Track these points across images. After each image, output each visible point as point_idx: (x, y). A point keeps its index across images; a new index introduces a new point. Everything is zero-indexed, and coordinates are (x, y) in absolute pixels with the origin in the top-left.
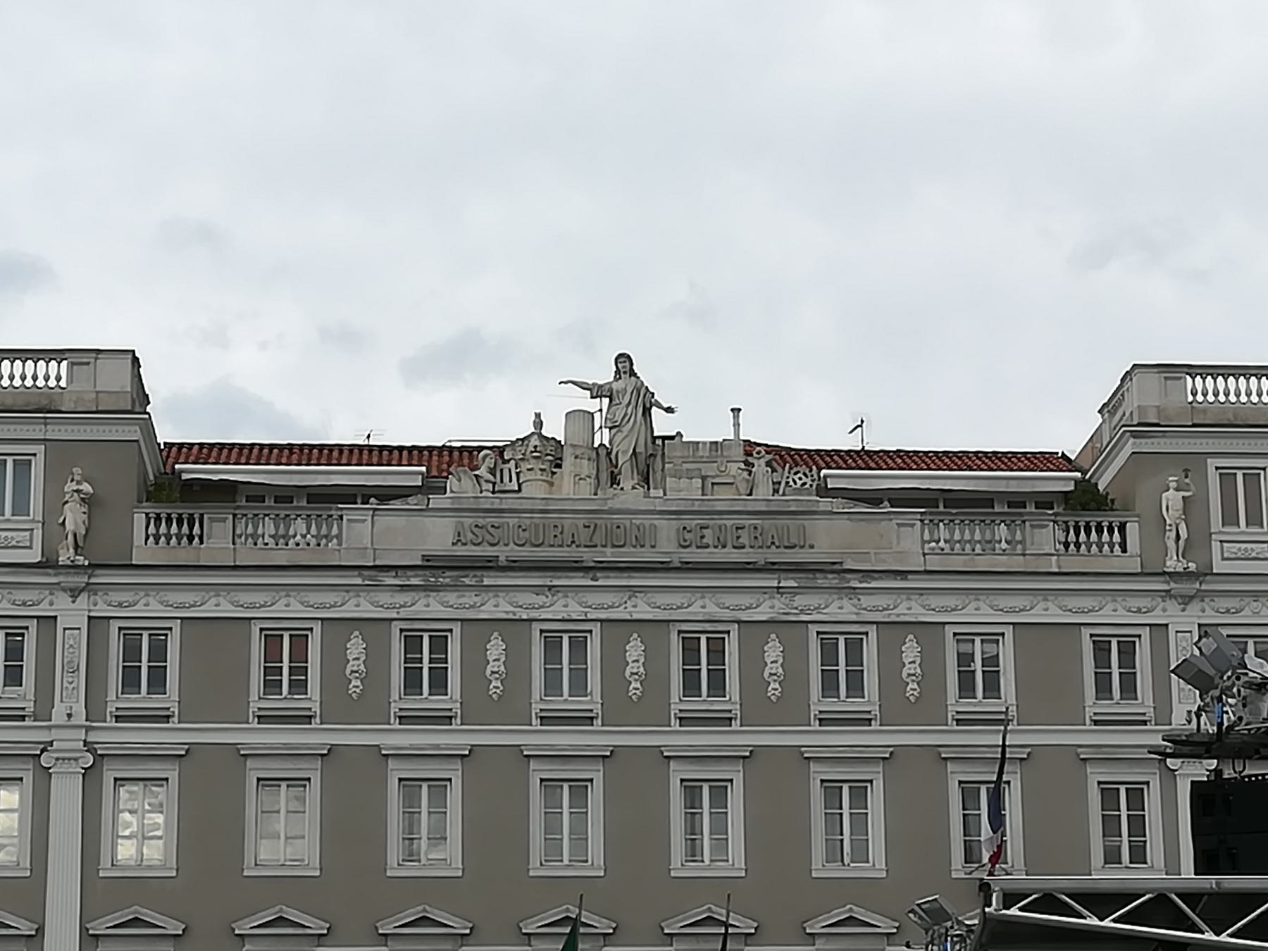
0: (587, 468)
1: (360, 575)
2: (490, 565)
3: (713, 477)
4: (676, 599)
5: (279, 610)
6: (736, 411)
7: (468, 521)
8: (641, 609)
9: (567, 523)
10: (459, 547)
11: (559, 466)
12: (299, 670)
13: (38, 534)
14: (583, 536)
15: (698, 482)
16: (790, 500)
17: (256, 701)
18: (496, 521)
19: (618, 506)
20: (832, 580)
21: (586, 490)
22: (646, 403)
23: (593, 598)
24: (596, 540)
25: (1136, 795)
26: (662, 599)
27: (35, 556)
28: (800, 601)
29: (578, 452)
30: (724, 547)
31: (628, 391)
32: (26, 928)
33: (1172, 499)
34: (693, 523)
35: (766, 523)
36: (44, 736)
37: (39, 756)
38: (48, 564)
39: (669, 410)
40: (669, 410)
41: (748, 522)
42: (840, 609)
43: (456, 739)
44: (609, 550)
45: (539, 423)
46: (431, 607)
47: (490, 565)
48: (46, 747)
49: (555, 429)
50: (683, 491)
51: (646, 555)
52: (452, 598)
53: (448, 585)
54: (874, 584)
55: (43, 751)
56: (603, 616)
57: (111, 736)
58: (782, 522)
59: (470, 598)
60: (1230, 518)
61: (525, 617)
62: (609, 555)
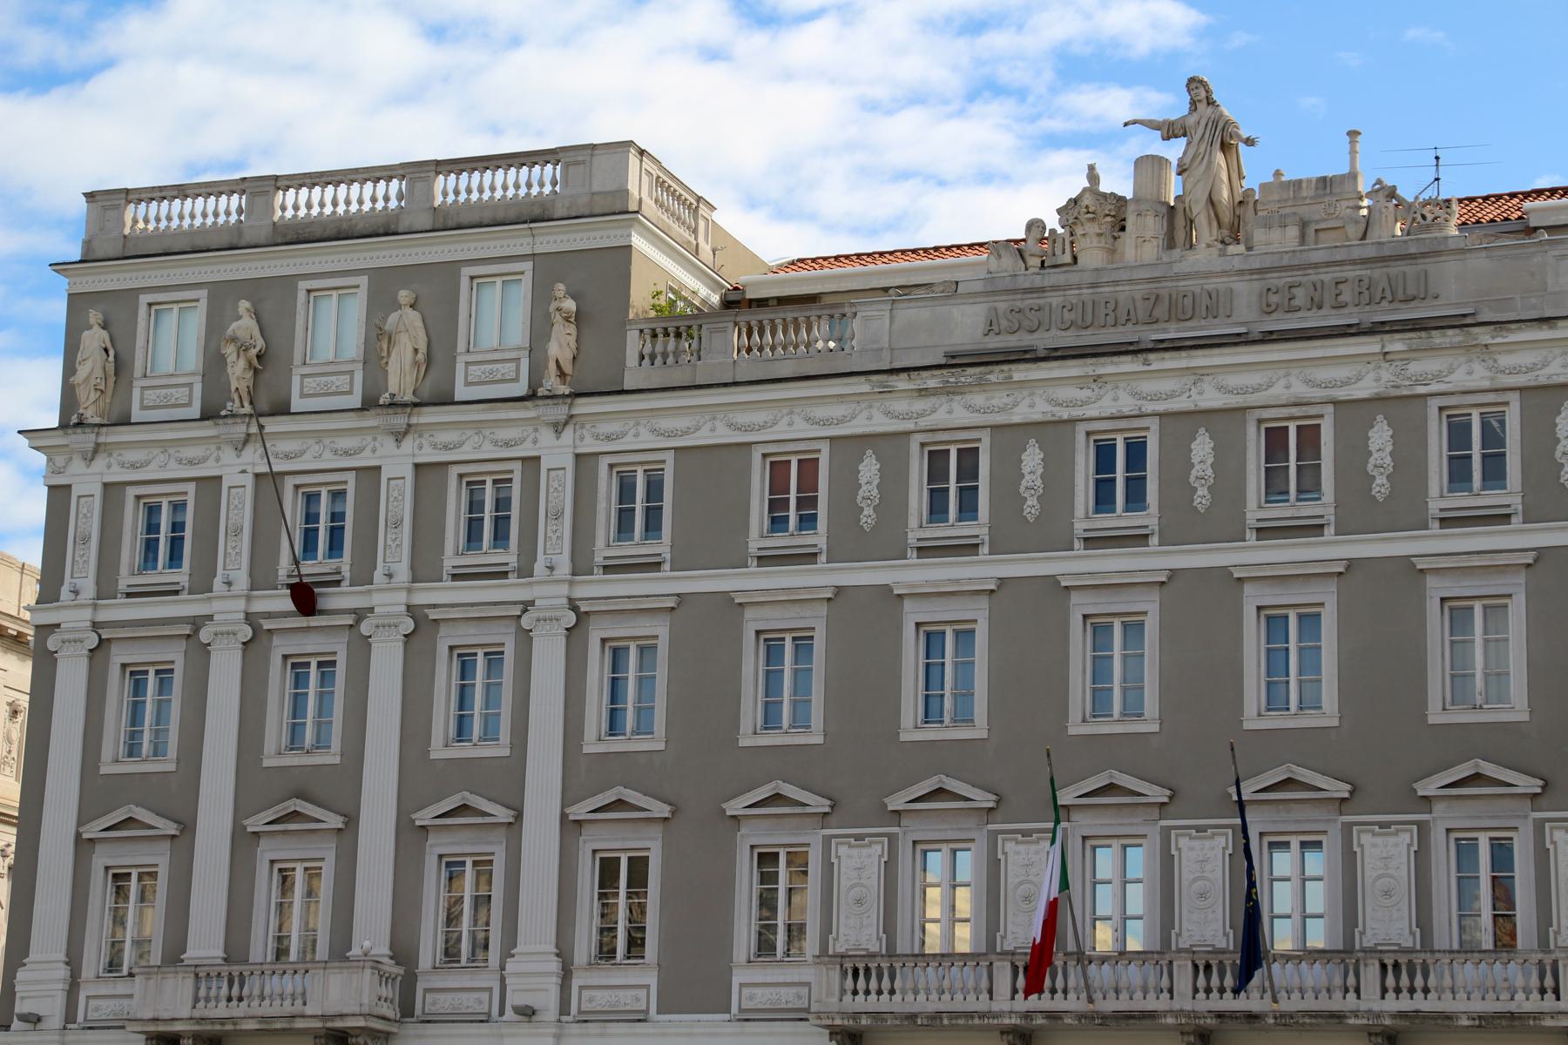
3: (1317, 222)
4: (1254, 379)
5: (781, 431)
6: (1353, 134)
7: (1002, 306)
8: (1210, 397)
11: (1123, 229)
13: (359, 377)
15: (1293, 232)
17: (757, 537)
19: (1188, 270)
20: (1453, 336)
21: (1150, 252)
22: (1225, 139)
23: (1147, 387)
24: (1157, 313)
26: (1234, 380)
27: (521, 389)
28: (1415, 368)
29: (1143, 207)
30: (1320, 308)
35: (1377, 273)
36: (523, 594)
37: (519, 617)
38: (532, 396)
39: (1250, 142)
41: (1351, 273)
43: (1334, 549)
44: (1173, 326)
45: (1093, 176)
48: (527, 605)
49: (1118, 182)
50: (1276, 241)
52: (978, 399)
54: (1512, 338)
55: (525, 611)
56: (1161, 407)
57: (594, 588)
58: (1396, 269)
59: (1000, 398)
61: (1065, 417)
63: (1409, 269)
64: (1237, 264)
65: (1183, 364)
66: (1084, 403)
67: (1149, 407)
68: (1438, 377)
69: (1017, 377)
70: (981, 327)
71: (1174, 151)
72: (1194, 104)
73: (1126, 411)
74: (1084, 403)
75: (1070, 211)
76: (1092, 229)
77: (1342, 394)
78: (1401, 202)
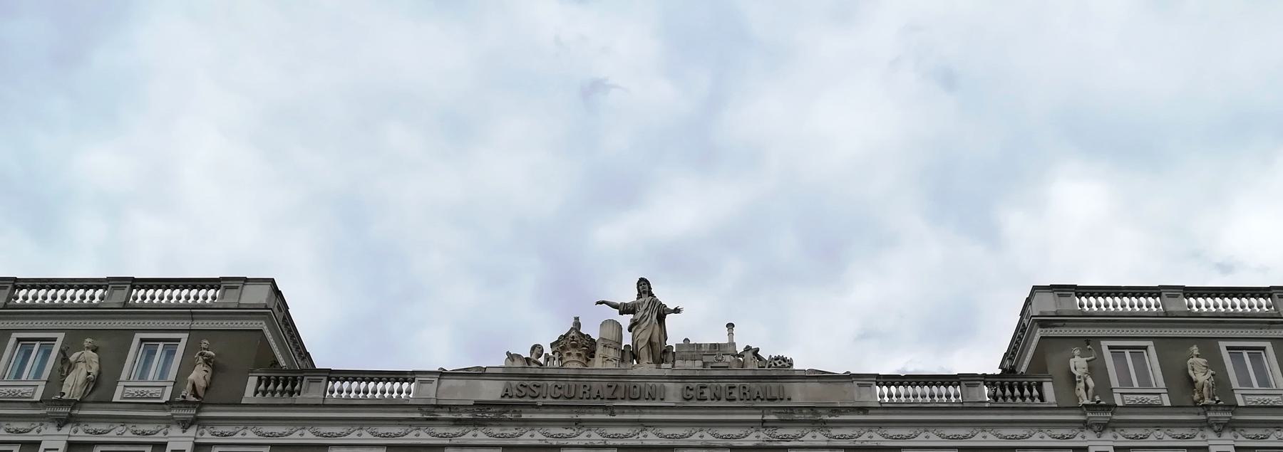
0: (612, 353)
1: (421, 412)
9: (594, 384)
10: (507, 399)
14: (607, 393)
18: (538, 383)
24: (617, 394)
28: (780, 432)
31: (649, 309)
33: (1078, 364)
34: (694, 385)
39: (677, 311)
40: (677, 311)
45: (577, 325)
49: (592, 330)
52: (496, 431)
53: (492, 420)
56: (619, 442)
59: (510, 431)
63: (774, 385)
64: (667, 373)
65: (636, 417)
66: (569, 436)
67: (611, 442)
68: (795, 438)
69: (524, 416)
71: (625, 320)
72: (640, 296)
73: (596, 443)
74: (569, 436)
75: (561, 345)
76: (574, 352)
77: (735, 443)
78: (760, 358)
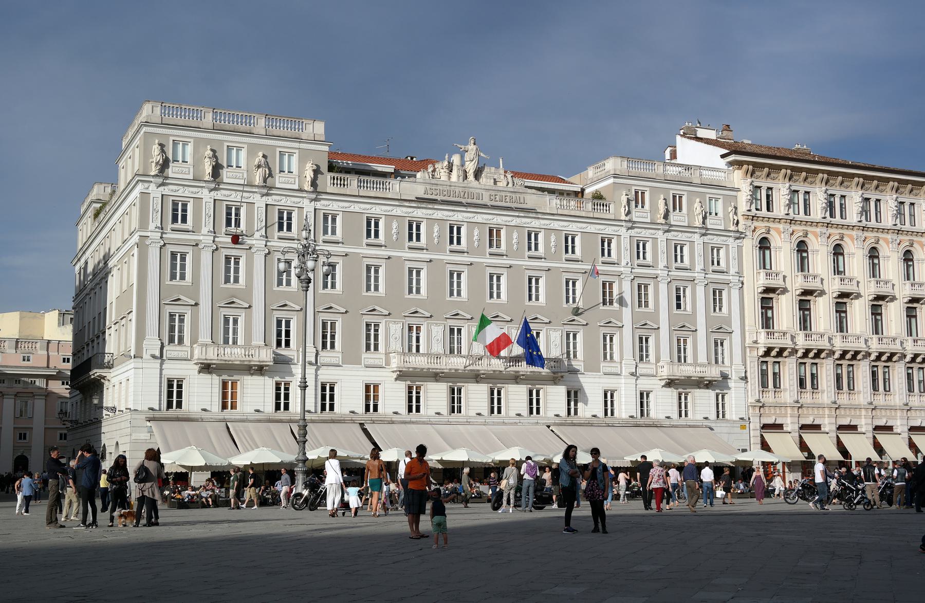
2: (434, 201)
12: (499, 241)
16: (517, 188)
20: (534, 215)
25: (646, 286)
32: (656, 326)
42: (535, 223)
46: (419, 213)
47: (434, 201)
51: (479, 202)
58: (518, 195)
60: (674, 209)
62: (469, 201)
70: (423, 192)
